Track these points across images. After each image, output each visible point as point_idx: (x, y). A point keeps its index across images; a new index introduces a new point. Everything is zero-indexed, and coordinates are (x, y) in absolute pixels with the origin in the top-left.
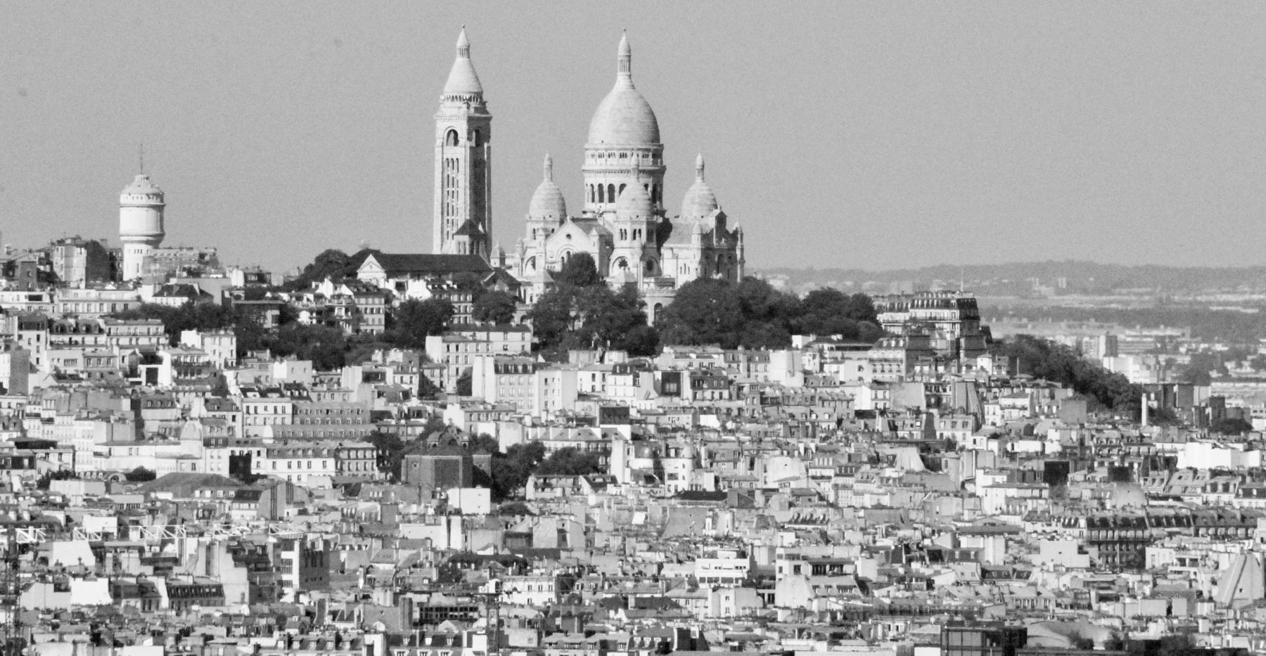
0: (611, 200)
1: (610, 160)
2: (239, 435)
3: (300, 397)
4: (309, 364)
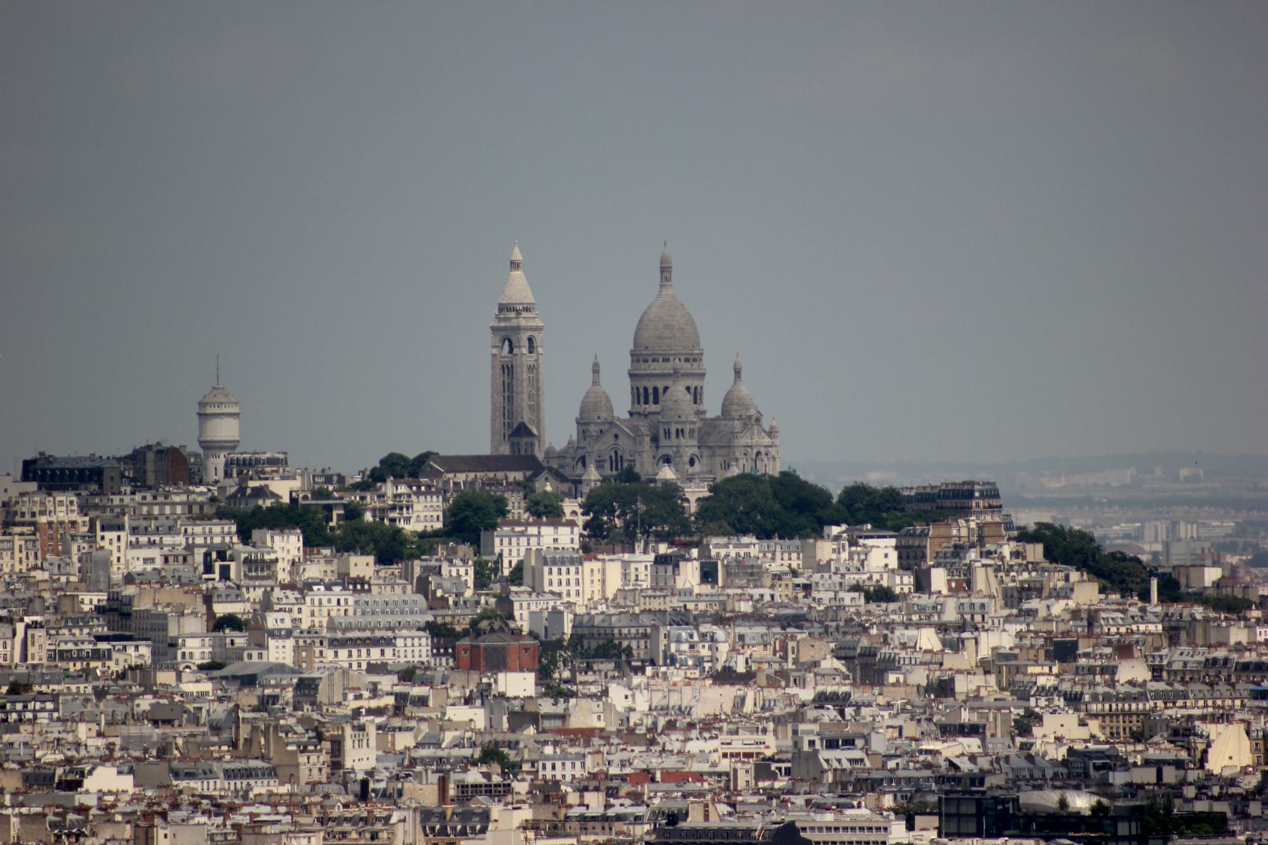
0: (656, 402)
1: (654, 365)
3: (363, 590)
4: (371, 559)
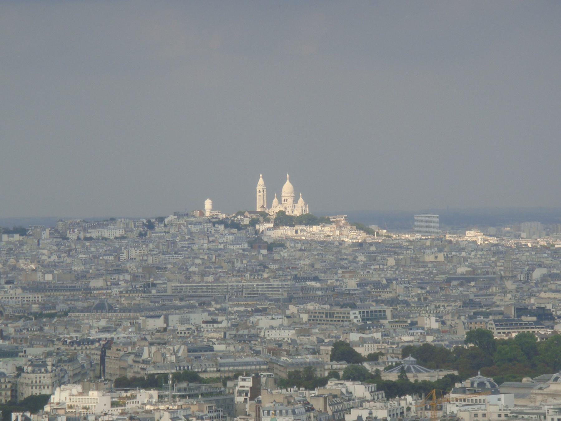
2: (225, 241)
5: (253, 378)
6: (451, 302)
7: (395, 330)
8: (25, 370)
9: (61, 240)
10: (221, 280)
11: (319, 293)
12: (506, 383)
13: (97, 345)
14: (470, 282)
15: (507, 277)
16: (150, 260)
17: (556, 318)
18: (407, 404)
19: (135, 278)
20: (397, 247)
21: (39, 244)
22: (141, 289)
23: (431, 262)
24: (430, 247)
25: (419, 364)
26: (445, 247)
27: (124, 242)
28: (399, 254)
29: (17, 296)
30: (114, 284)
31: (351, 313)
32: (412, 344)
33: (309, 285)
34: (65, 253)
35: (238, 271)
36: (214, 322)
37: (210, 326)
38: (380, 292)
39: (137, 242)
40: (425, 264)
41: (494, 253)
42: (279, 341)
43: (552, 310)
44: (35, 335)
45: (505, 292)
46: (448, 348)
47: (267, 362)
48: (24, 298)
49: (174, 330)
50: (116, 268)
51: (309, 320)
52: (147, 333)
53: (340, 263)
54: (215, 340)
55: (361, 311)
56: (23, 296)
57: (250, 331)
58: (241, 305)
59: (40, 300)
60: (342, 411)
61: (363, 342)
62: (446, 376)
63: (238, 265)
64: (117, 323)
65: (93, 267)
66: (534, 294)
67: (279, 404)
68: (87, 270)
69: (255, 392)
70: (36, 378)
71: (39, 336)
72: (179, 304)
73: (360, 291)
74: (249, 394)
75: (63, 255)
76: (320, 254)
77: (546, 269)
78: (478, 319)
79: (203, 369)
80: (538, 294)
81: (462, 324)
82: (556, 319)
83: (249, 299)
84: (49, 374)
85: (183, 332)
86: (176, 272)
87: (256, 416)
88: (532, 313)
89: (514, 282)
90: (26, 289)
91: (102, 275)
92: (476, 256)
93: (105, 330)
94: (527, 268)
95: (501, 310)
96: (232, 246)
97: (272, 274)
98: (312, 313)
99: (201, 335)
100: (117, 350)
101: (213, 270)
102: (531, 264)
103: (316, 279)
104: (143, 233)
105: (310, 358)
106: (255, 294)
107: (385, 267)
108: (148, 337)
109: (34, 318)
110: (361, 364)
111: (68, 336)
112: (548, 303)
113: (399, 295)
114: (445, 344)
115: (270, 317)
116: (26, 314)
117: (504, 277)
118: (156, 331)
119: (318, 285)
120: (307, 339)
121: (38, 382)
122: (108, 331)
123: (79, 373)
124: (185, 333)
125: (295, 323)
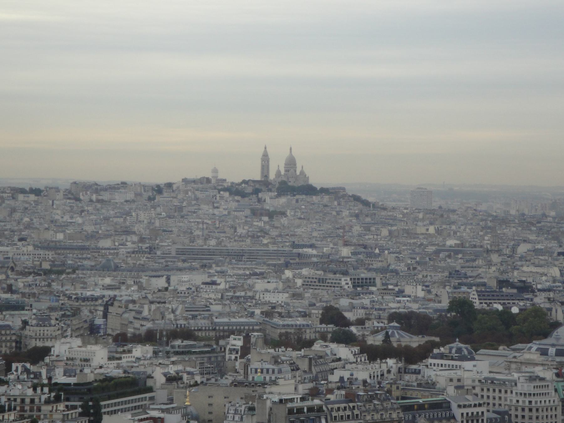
5: (244, 337)
6: (439, 273)
7: (383, 297)
8: (29, 323)
9: (74, 201)
10: (223, 244)
11: (315, 260)
12: (482, 351)
13: (100, 301)
14: (458, 254)
15: (493, 250)
16: (157, 224)
17: (536, 291)
18: (387, 367)
19: (142, 240)
20: (391, 219)
21: (53, 205)
22: (146, 250)
23: (423, 234)
24: (423, 220)
25: (403, 330)
26: (437, 220)
27: (134, 206)
28: (392, 225)
29: (29, 253)
30: (122, 245)
31: (343, 279)
32: (397, 311)
33: (306, 252)
34: (78, 213)
35: (240, 236)
36: (214, 283)
37: (209, 287)
38: (373, 261)
39: (146, 205)
40: (415, 235)
41: (482, 228)
42: (272, 303)
43: (533, 283)
44: (42, 290)
45: (490, 264)
46: (431, 316)
47: (260, 323)
48: (35, 254)
49: (175, 290)
50: (125, 229)
51: (303, 285)
52: (149, 292)
53: (336, 233)
54: (213, 301)
55: (353, 277)
56: (34, 253)
57: (246, 293)
58: (240, 269)
59: (50, 258)
60: (326, 371)
61: (352, 307)
62: (427, 342)
63: (240, 231)
64: (122, 281)
65: (103, 228)
66: (518, 267)
67: (266, 363)
68: (97, 230)
69: (245, 351)
70: (40, 331)
71: (46, 292)
72: (181, 266)
73: (353, 259)
74: (239, 353)
75: (75, 216)
76: (318, 223)
77: (530, 244)
78: (462, 289)
79: (199, 328)
80: (521, 268)
81: (447, 293)
82: (536, 292)
83: (248, 263)
84: (52, 328)
85: (183, 292)
86: (181, 235)
87: (245, 374)
88: (513, 286)
89: (499, 256)
90: (38, 247)
91: (111, 235)
92: (465, 230)
93: (110, 287)
94: (512, 243)
95: (485, 282)
96: (236, 213)
97: (272, 240)
98: (306, 278)
99: (200, 295)
100: (119, 307)
101: (217, 235)
102: (517, 239)
103: (312, 246)
104: (152, 197)
105: (300, 321)
106: (255, 258)
107: (379, 237)
108: (150, 297)
109: (43, 274)
110: (349, 328)
111: (74, 292)
112: (529, 277)
113: (390, 265)
114: (429, 312)
115: (266, 281)
116: (36, 271)
117: (490, 251)
118: (157, 290)
119: (314, 252)
120: (300, 302)
121: (42, 335)
122: (112, 289)
123: (82, 327)
124: (185, 293)
125: (290, 287)
